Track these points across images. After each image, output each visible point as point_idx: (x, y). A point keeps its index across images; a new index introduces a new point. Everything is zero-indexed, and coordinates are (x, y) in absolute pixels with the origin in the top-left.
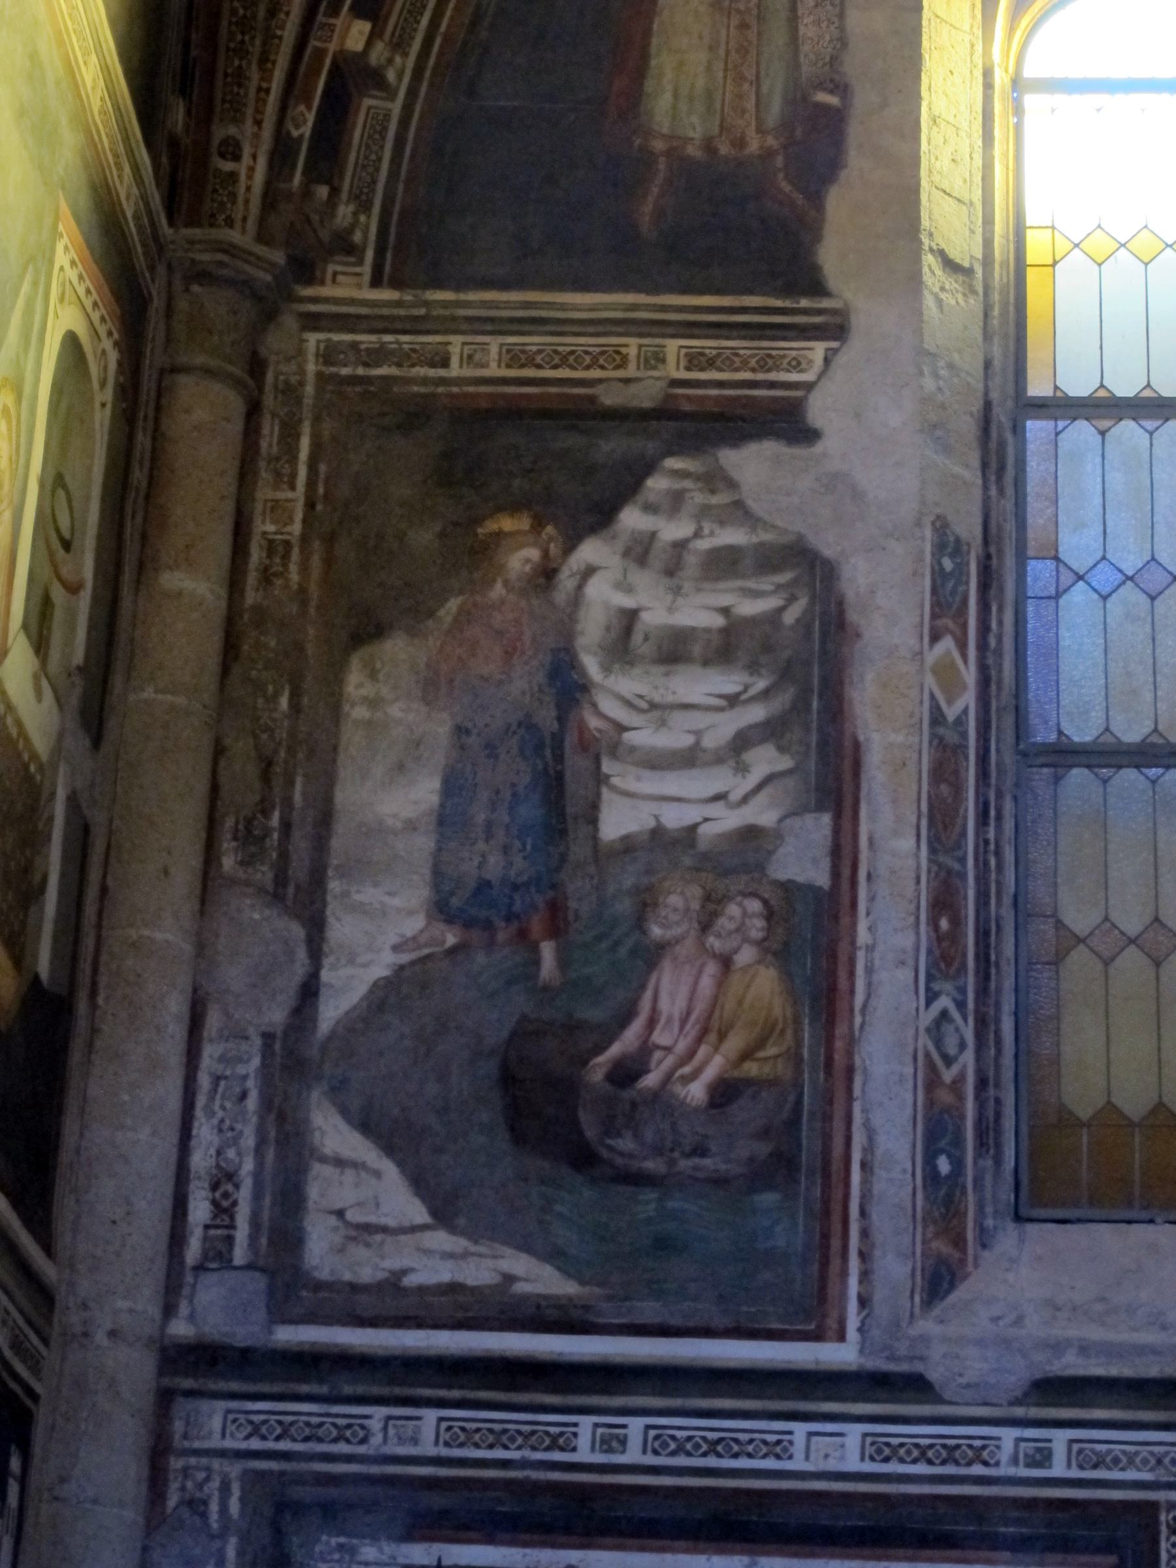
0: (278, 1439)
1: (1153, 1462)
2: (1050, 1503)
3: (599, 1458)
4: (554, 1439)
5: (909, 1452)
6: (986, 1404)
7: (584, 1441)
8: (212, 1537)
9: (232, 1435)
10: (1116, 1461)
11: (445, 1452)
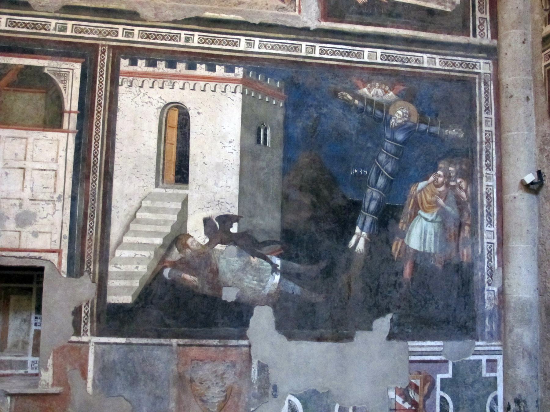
1: (98, 32)
2: (65, 42)
5: (21, 25)
6: (47, 12)
10: (87, 31)
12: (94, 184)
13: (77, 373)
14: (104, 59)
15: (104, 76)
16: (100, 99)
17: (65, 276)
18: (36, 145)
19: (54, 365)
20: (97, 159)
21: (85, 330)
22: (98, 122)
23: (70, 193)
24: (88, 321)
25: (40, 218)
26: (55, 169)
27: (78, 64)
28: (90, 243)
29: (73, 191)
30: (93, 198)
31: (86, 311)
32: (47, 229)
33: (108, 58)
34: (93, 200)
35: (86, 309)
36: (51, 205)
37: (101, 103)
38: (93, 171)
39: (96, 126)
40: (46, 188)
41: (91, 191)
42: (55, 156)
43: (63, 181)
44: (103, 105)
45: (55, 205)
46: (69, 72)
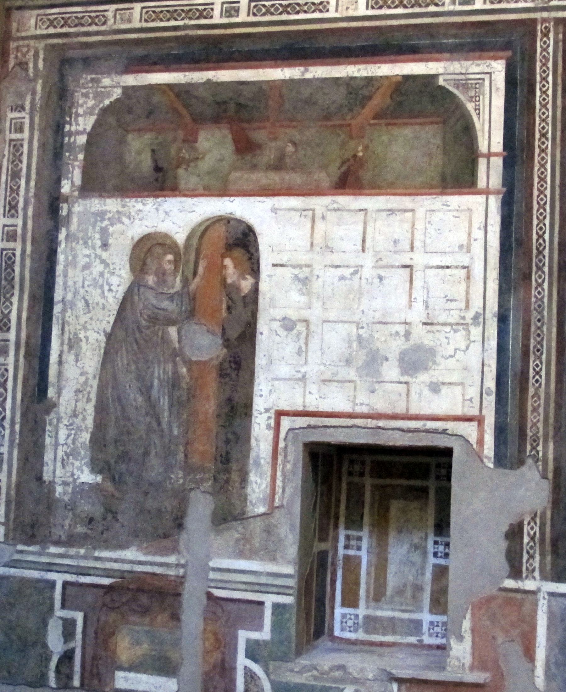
0: (62, 27)
2: (473, 24)
3: (225, 21)
4: (201, 12)
7: (217, 12)
8: (30, 80)
9: (40, 27)
11: (145, 25)
12: (540, 289)
13: (517, 648)
14: (548, 46)
15: (550, 79)
16: (543, 124)
17: (491, 465)
18: (429, 222)
19: (473, 631)
20: (544, 241)
21: (530, 568)
22: (543, 170)
23: (496, 309)
24: (535, 552)
25: (442, 356)
26: (466, 265)
27: (499, 61)
28: (535, 402)
29: (500, 306)
30: (539, 317)
31: (532, 533)
32: (454, 378)
33: (556, 43)
34: (539, 320)
35: (532, 528)
36: (463, 333)
37: (547, 132)
38: (537, 265)
39: (539, 177)
40: (451, 301)
41: (536, 302)
42: (465, 243)
43: (482, 285)
44: (549, 135)
45: (469, 332)
46: (483, 79)
